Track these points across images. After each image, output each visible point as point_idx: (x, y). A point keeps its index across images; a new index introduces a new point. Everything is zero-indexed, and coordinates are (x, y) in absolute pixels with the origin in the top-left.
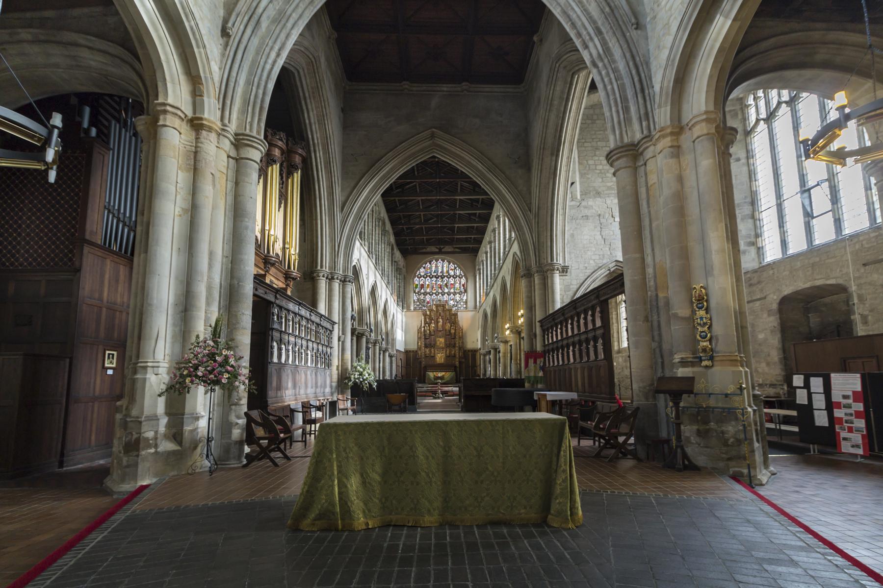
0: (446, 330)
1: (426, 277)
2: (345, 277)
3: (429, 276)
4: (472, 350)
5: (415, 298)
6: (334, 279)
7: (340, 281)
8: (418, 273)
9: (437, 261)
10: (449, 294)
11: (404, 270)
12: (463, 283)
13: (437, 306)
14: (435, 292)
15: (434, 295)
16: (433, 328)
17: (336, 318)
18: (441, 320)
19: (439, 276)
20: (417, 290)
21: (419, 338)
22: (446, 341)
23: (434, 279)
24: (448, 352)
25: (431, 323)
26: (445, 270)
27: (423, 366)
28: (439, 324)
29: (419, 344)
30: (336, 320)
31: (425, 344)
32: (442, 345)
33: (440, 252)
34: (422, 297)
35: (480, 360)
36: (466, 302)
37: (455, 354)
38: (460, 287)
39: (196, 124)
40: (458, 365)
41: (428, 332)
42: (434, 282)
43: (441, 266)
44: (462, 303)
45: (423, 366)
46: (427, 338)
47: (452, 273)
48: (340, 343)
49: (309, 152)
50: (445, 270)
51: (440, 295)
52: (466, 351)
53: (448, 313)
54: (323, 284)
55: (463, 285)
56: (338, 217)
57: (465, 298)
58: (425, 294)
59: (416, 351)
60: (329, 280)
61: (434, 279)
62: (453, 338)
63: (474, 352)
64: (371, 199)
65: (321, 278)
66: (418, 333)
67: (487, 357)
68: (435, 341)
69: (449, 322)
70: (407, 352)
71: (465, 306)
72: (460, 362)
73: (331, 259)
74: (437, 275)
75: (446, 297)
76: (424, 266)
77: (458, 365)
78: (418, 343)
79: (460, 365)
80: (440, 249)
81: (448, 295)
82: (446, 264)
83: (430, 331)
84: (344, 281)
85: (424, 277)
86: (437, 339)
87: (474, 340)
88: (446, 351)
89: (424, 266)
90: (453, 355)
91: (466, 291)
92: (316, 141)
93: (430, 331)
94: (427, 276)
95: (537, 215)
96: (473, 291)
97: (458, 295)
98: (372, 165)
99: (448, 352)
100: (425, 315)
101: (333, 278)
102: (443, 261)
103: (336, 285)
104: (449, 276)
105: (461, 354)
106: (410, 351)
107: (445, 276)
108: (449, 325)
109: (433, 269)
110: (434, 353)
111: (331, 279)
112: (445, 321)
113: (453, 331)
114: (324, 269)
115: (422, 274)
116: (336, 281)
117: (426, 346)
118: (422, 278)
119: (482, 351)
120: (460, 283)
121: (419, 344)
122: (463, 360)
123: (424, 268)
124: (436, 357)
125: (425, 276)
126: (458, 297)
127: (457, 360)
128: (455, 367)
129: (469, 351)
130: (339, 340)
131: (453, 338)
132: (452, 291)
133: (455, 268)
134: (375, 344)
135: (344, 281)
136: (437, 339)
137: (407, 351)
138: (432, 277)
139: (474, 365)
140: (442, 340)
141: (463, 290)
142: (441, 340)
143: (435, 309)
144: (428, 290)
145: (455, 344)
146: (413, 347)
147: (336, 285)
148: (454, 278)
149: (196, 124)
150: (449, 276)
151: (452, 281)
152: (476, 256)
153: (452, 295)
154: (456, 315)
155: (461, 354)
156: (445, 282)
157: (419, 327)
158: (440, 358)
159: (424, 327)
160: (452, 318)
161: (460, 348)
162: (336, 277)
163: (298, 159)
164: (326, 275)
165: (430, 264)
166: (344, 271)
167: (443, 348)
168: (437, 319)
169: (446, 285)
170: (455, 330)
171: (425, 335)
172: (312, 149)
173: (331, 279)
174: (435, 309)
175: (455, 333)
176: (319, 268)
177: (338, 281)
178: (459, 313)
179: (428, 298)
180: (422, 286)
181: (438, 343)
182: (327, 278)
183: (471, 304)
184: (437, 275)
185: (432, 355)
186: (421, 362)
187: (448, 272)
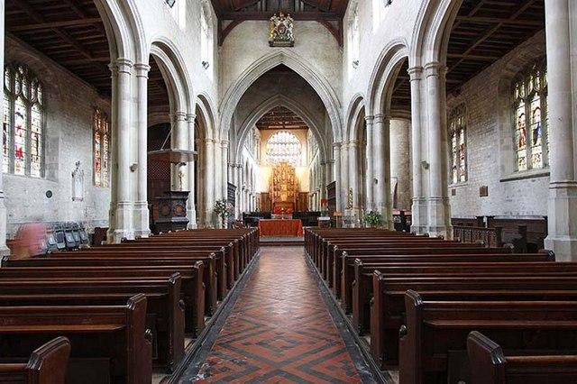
30: (236, 184)
33: (284, 128)
39: (214, 142)
43: (283, 136)
46: (275, 185)
50: (287, 138)
56: (236, 137)
67: (314, 198)
75: (286, 158)
80: (284, 124)
84: (238, 167)
87: (305, 187)
95: (327, 137)
98: (252, 112)
103: (236, 169)
109: (280, 137)
117: (275, 190)
119: (310, 194)
126: (295, 157)
132: (292, 153)
134: (246, 192)
135: (238, 167)
139: (306, 202)
146: (265, 190)
147: (236, 169)
149: (214, 142)
154: (294, 169)
158: (284, 197)
160: (292, 172)
161: (297, 191)
173: (233, 167)
179: (276, 158)
183: (304, 163)
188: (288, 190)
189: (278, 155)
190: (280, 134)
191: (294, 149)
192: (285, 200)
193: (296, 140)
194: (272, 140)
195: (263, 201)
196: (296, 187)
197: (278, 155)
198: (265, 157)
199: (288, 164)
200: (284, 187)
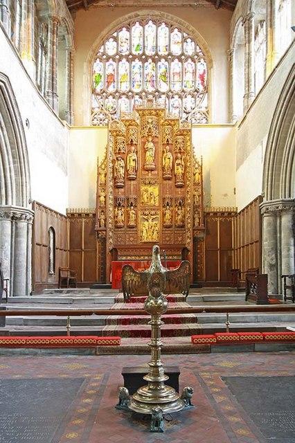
0: (163, 168)
1: (120, 60)
3: (127, 57)
4: (223, 213)
5: (95, 104)
8: (101, 51)
9: (143, 23)
10: (170, 94)
11: (69, 38)
12: (201, 72)
13: (142, 113)
14: (136, 90)
15: (137, 97)
16: (133, 164)
18: (150, 145)
19: (147, 57)
20: (98, 89)
21: (102, 186)
22: (162, 191)
23: (137, 63)
24: (168, 216)
25: (129, 152)
26: (163, 42)
27: (109, 247)
28: (148, 154)
29: (102, 199)
31: (116, 199)
32: (156, 202)
34: (110, 102)
35: (242, 233)
36: (206, 115)
37: (183, 222)
38: (194, 82)
40: (190, 247)
41: (122, 171)
42: (136, 70)
44: (198, 116)
45: (109, 247)
47: (176, 50)
50: (163, 42)
51: (150, 97)
52: (208, 214)
53: (167, 129)
55: (202, 77)
57: (205, 103)
58: (118, 95)
59: (94, 215)
61: (137, 63)
62: (181, 187)
63: (229, 216)
66: (99, 174)
68: (137, 191)
69: (170, 151)
70: (72, 216)
71: (204, 121)
72: (195, 240)
74: (144, 54)
76: (115, 35)
77: (190, 247)
78: (99, 197)
79: (195, 245)
81: (168, 97)
82: (163, 29)
83: (127, 171)
85: (114, 60)
86: (143, 188)
88: (164, 215)
89: (115, 35)
90: (179, 223)
91: (206, 89)
93: (127, 171)
94: (121, 57)
96: (224, 87)
97: (189, 97)
99: (168, 216)
100: (115, 133)
102: (157, 23)
104: (170, 57)
105: (197, 220)
106: (80, 215)
107: (160, 57)
108: (169, 155)
109: (136, 41)
110: (136, 220)
112: (161, 149)
113: (179, 170)
115: (111, 52)
117: (117, 205)
118: (111, 61)
120: (194, 73)
121: (102, 199)
122: (202, 235)
123: (116, 39)
124: (140, 227)
125: (118, 58)
126: (189, 102)
127: (189, 234)
128: (185, 250)
129: (215, 214)
131: (181, 187)
132: (177, 88)
133: (184, 40)
136: (143, 188)
137: (73, 215)
138: (133, 60)
139: (227, 248)
140: (155, 190)
141: (201, 88)
142: (151, 189)
143: (138, 121)
144: (124, 87)
145: (184, 199)
148: (180, 60)
150: (170, 57)
151: (176, 66)
152: (230, 18)
153: (176, 97)
154: (186, 133)
155: (197, 220)
156: (163, 70)
157: (101, 160)
158: (149, 230)
159: (113, 161)
160: (179, 141)
161: (195, 208)
165: (129, 30)
167: (153, 208)
168: (144, 143)
169: (165, 76)
170: (186, 167)
171: (115, 179)
174: (138, 121)
175: (183, 174)
178: (194, 131)
179: (124, 105)
180: (110, 79)
181: (145, 196)
183: (218, 115)
184: (144, 54)
185: (132, 223)
186: (104, 241)
187: (168, 47)
188: (165, 203)
189: (129, 95)
190: (137, 29)
191: (188, 75)
192: (155, 237)
193: (190, 48)
194: (110, 47)
195: (74, 246)
196: (191, 194)
197: (129, 95)
198: (85, 103)
199: (172, 123)
200: (151, 193)
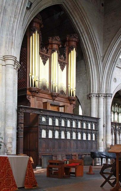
2: (107, 94)
6: (100, 96)
7: (104, 97)
17: (102, 116)
48: (105, 128)
49: (79, 38)
54: (94, 100)
60: (98, 97)
64: (112, 48)
65: (93, 97)
73: (98, 87)
84: (106, 97)
92: (82, 31)
101: (99, 96)
103: (102, 100)
111: (98, 96)
114: (94, 92)
116: (101, 97)
130: (104, 127)
147: (102, 100)
162: (100, 95)
163: (73, 43)
164: (95, 95)
166: (106, 91)
172: (81, 35)
173: (98, 96)
176: (92, 92)
177: (103, 97)
182: (96, 96)
